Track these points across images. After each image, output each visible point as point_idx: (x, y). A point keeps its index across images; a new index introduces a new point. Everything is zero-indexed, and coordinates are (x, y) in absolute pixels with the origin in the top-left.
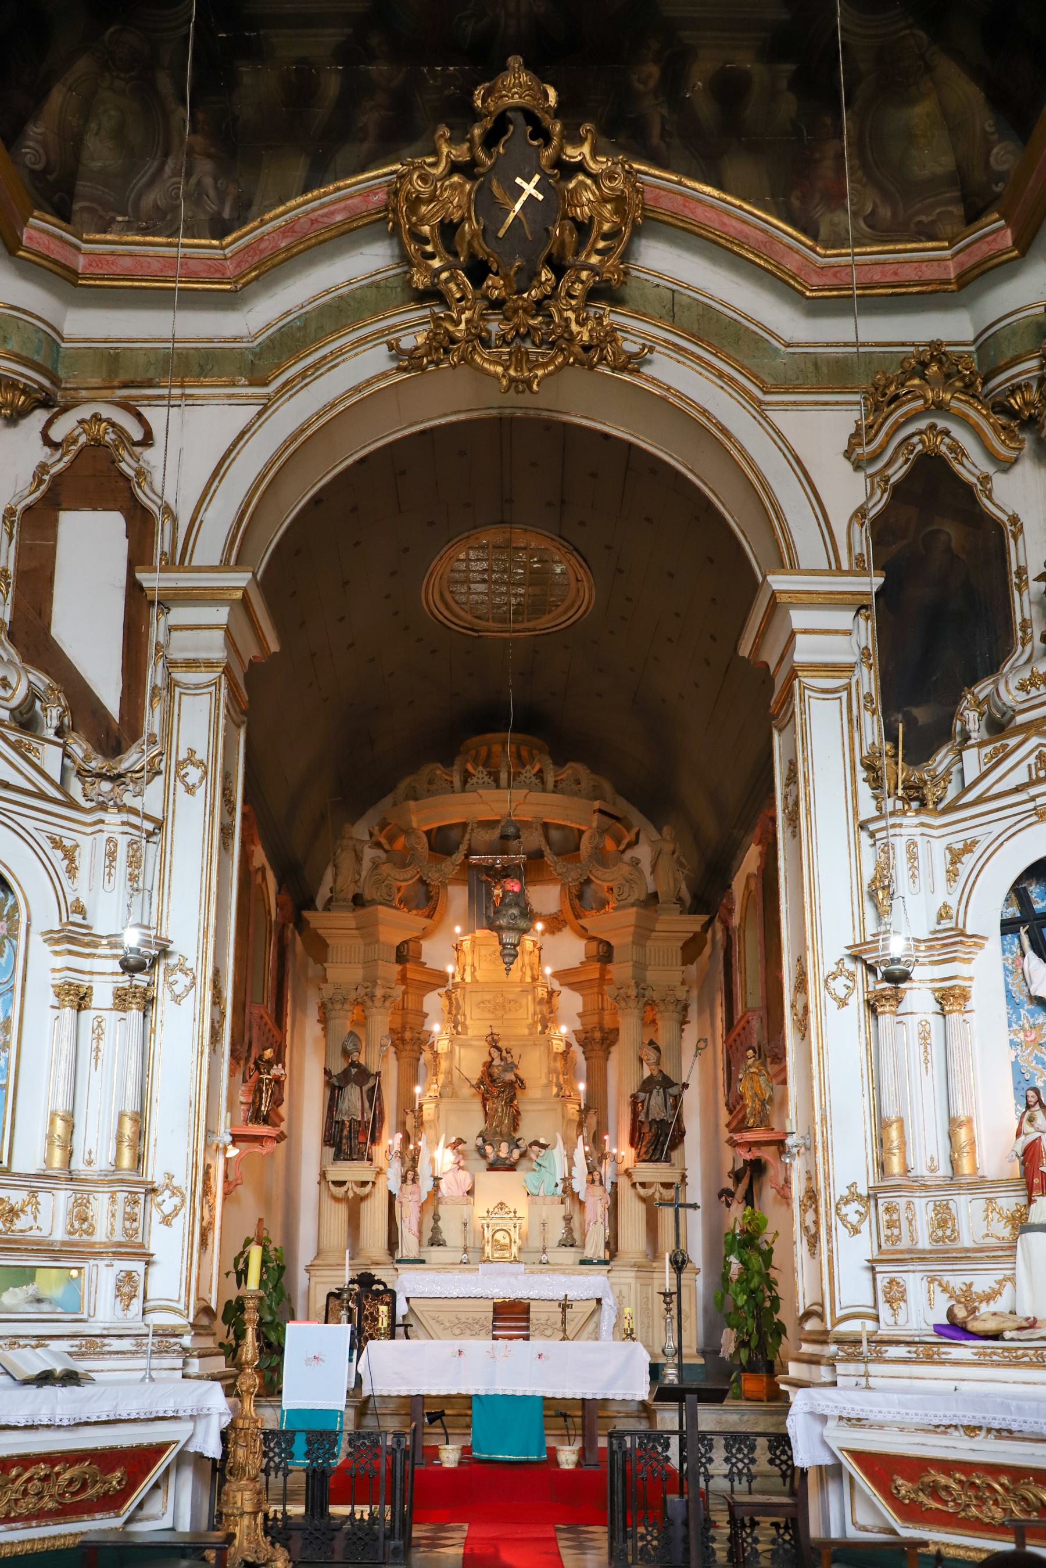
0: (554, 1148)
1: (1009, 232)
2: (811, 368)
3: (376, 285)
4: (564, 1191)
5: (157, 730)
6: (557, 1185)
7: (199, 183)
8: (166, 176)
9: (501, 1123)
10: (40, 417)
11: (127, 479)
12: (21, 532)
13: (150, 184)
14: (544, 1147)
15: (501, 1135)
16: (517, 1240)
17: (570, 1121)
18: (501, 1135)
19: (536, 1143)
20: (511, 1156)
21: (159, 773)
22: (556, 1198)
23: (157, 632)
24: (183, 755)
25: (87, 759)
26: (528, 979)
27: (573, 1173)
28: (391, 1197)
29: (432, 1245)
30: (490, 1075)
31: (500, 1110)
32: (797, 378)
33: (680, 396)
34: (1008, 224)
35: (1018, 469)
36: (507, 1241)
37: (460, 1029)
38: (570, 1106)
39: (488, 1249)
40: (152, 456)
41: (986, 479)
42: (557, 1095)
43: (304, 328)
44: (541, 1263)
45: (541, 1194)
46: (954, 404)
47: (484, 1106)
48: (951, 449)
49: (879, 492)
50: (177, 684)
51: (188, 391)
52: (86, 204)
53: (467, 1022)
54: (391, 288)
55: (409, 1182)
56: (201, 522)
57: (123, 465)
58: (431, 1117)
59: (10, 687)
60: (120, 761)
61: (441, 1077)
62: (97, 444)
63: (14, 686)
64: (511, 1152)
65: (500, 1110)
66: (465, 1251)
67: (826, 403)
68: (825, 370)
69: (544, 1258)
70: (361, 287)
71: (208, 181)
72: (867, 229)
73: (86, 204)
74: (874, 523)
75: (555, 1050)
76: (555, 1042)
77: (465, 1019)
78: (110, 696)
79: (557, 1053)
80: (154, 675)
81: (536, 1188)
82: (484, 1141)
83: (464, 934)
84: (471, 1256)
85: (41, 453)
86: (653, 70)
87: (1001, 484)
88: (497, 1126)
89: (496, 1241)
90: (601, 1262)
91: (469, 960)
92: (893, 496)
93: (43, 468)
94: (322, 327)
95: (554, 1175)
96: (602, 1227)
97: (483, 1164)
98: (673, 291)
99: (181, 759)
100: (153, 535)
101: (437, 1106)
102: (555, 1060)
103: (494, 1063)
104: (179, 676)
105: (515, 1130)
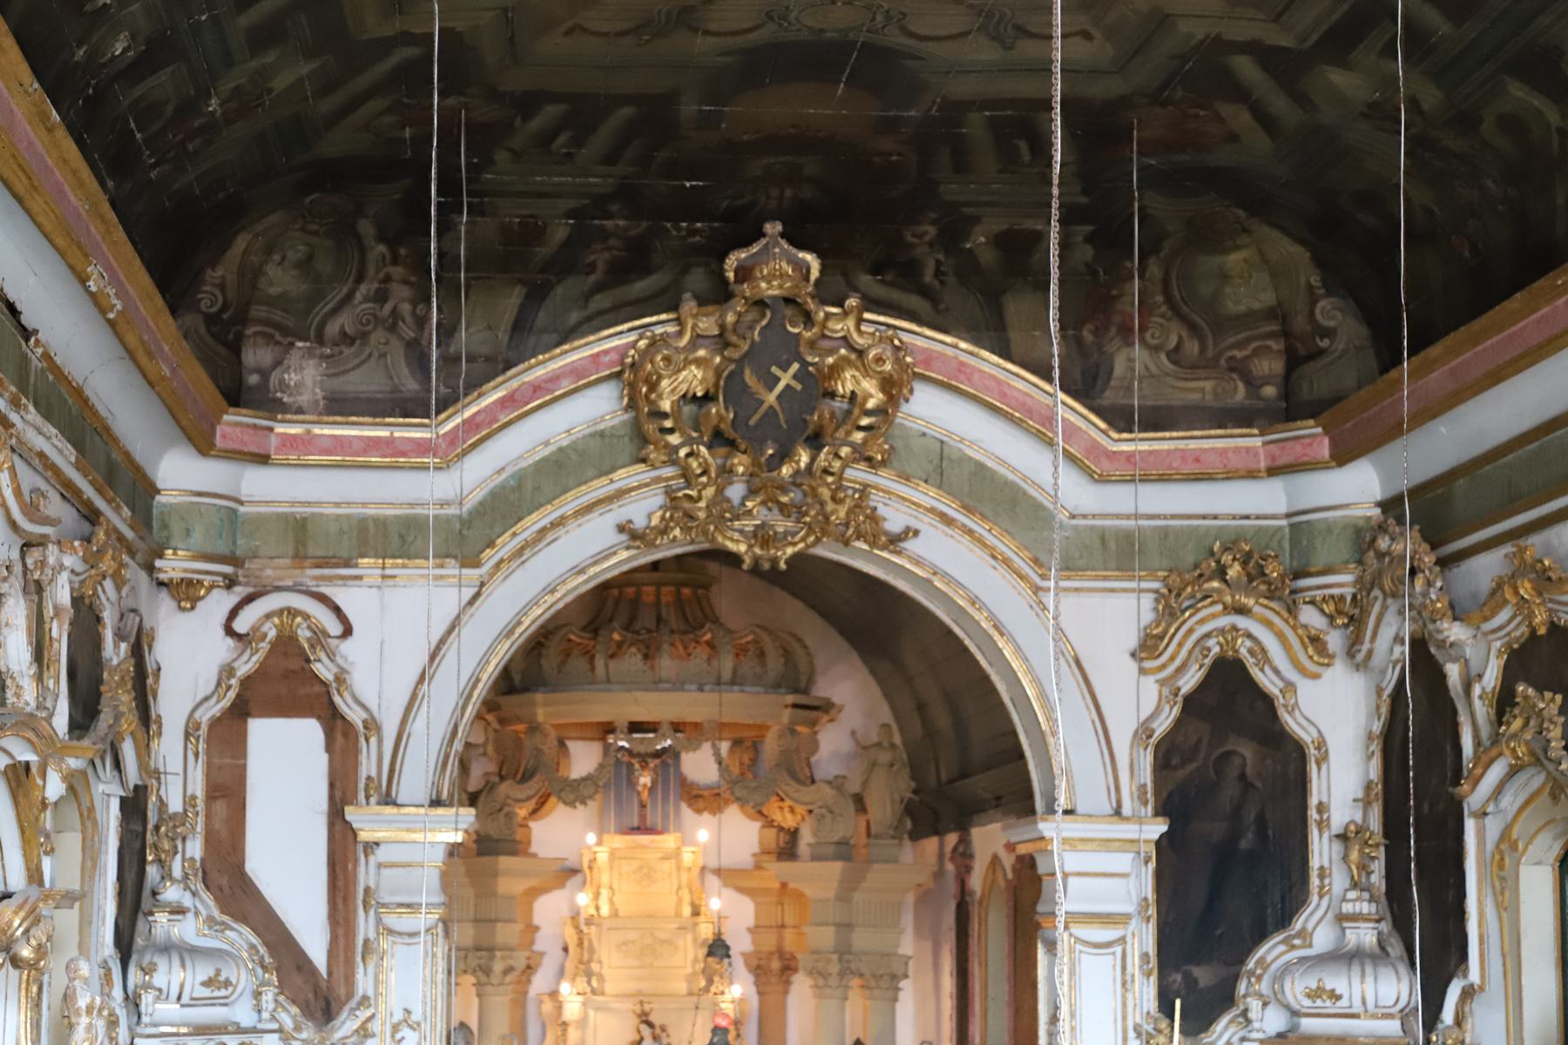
1: (1326, 441)
2: (1097, 543)
3: (602, 434)
5: (370, 993)
7: (394, 311)
8: (356, 301)
10: (218, 603)
11: (324, 684)
12: (208, 752)
13: (335, 311)
21: (373, 1035)
23: (366, 875)
24: (398, 1016)
25: (298, 1028)
26: (687, 911)
32: (1081, 557)
33: (945, 576)
34: (1326, 432)
35: (1328, 674)
40: (347, 648)
41: (1290, 687)
43: (519, 487)
46: (1257, 609)
48: (1251, 652)
49: (1167, 708)
50: (391, 932)
51: (388, 572)
52: (259, 328)
54: (618, 437)
56: (409, 735)
57: (318, 668)
59: (231, 984)
60: (333, 1030)
62: (286, 644)
63: (234, 982)
67: (1113, 590)
68: (1112, 546)
70: (584, 437)
71: (406, 308)
72: (1171, 366)
73: (259, 328)
74: (1157, 747)
78: (316, 946)
80: (365, 926)
83: (600, 843)
85: (223, 648)
86: (932, 231)
87: (1305, 687)
91: (605, 879)
92: (1184, 710)
93: (228, 671)
94: (537, 489)
98: (942, 442)
99: (395, 1020)
100: (356, 751)
104: (391, 920)
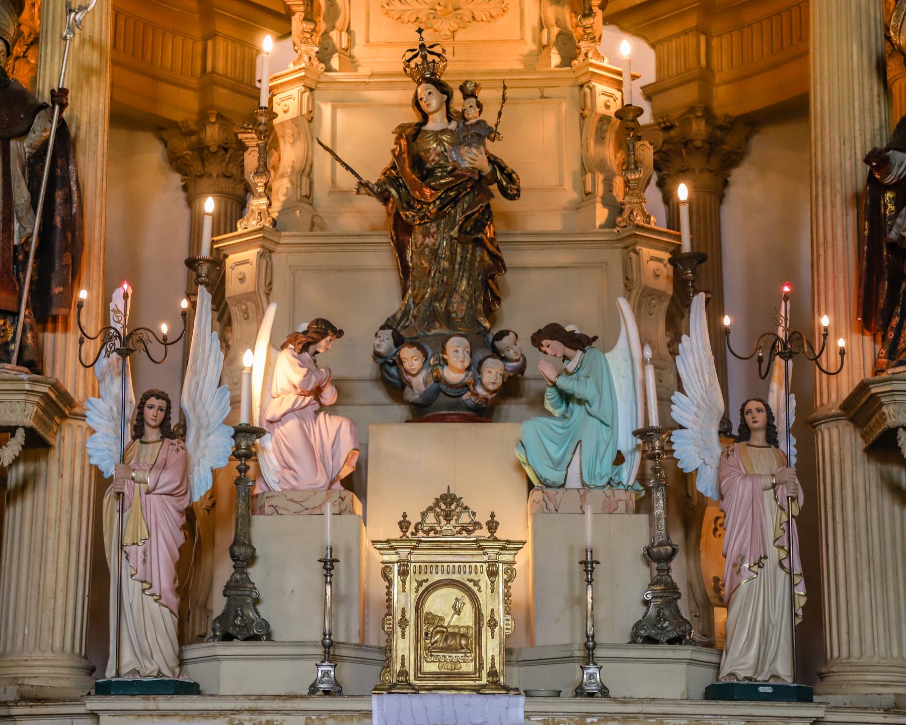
0: (609, 347)
4: (642, 478)
6: (619, 459)
9: (448, 290)
14: (579, 342)
15: (448, 319)
16: (500, 616)
17: (650, 293)
18: (448, 319)
19: (554, 332)
20: (478, 381)
22: (620, 494)
27: (678, 413)
28: (101, 482)
29: (227, 637)
30: (418, 163)
31: (444, 252)
36: (467, 618)
37: (335, 62)
38: (647, 252)
39: (403, 646)
42: (611, 223)
44: (580, 692)
45: (574, 482)
47: (400, 249)
53: (356, 51)
55: (152, 434)
58: (249, 286)
61: (282, 187)
64: (476, 367)
65: (444, 252)
66: (333, 655)
69: (593, 675)
75: (601, 109)
76: (600, 87)
77: (351, 41)
79: (604, 119)
81: (556, 465)
82: (399, 341)
84: (348, 673)
88: (435, 297)
89: (432, 619)
90: (781, 694)
95: (608, 424)
96: (782, 575)
97: (400, 411)
101: (266, 254)
102: (600, 137)
103: (431, 126)
105: (490, 313)
